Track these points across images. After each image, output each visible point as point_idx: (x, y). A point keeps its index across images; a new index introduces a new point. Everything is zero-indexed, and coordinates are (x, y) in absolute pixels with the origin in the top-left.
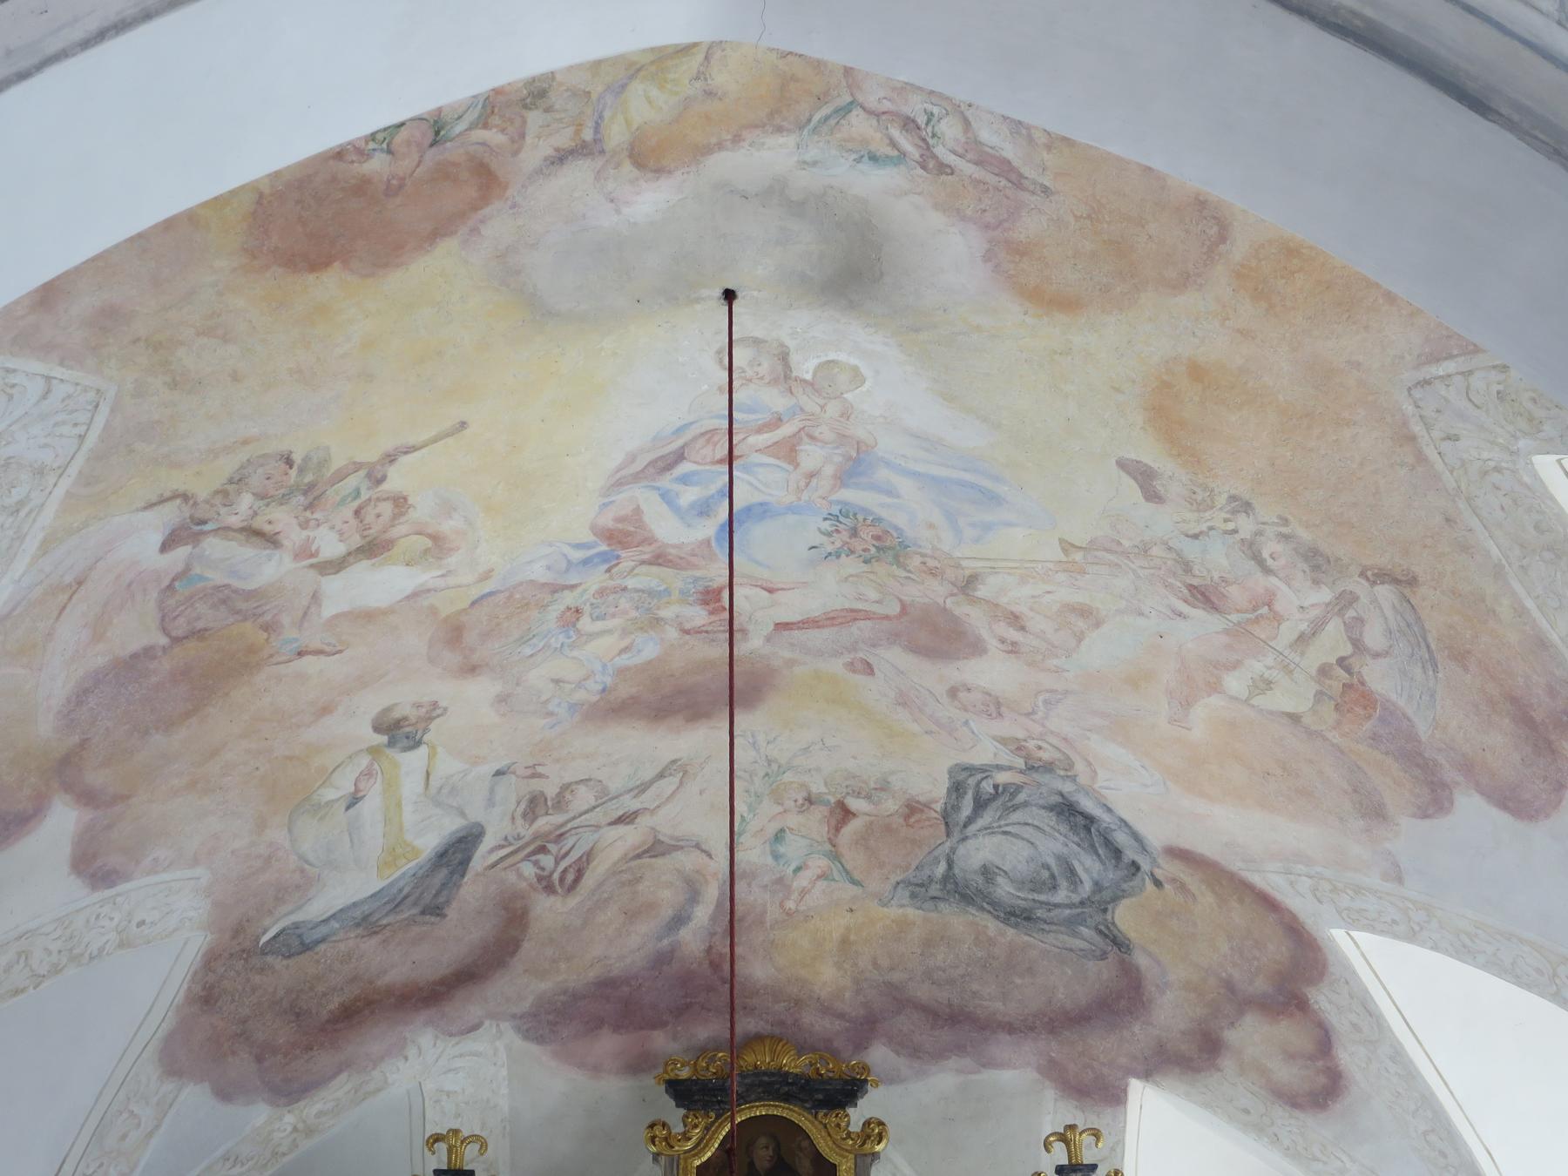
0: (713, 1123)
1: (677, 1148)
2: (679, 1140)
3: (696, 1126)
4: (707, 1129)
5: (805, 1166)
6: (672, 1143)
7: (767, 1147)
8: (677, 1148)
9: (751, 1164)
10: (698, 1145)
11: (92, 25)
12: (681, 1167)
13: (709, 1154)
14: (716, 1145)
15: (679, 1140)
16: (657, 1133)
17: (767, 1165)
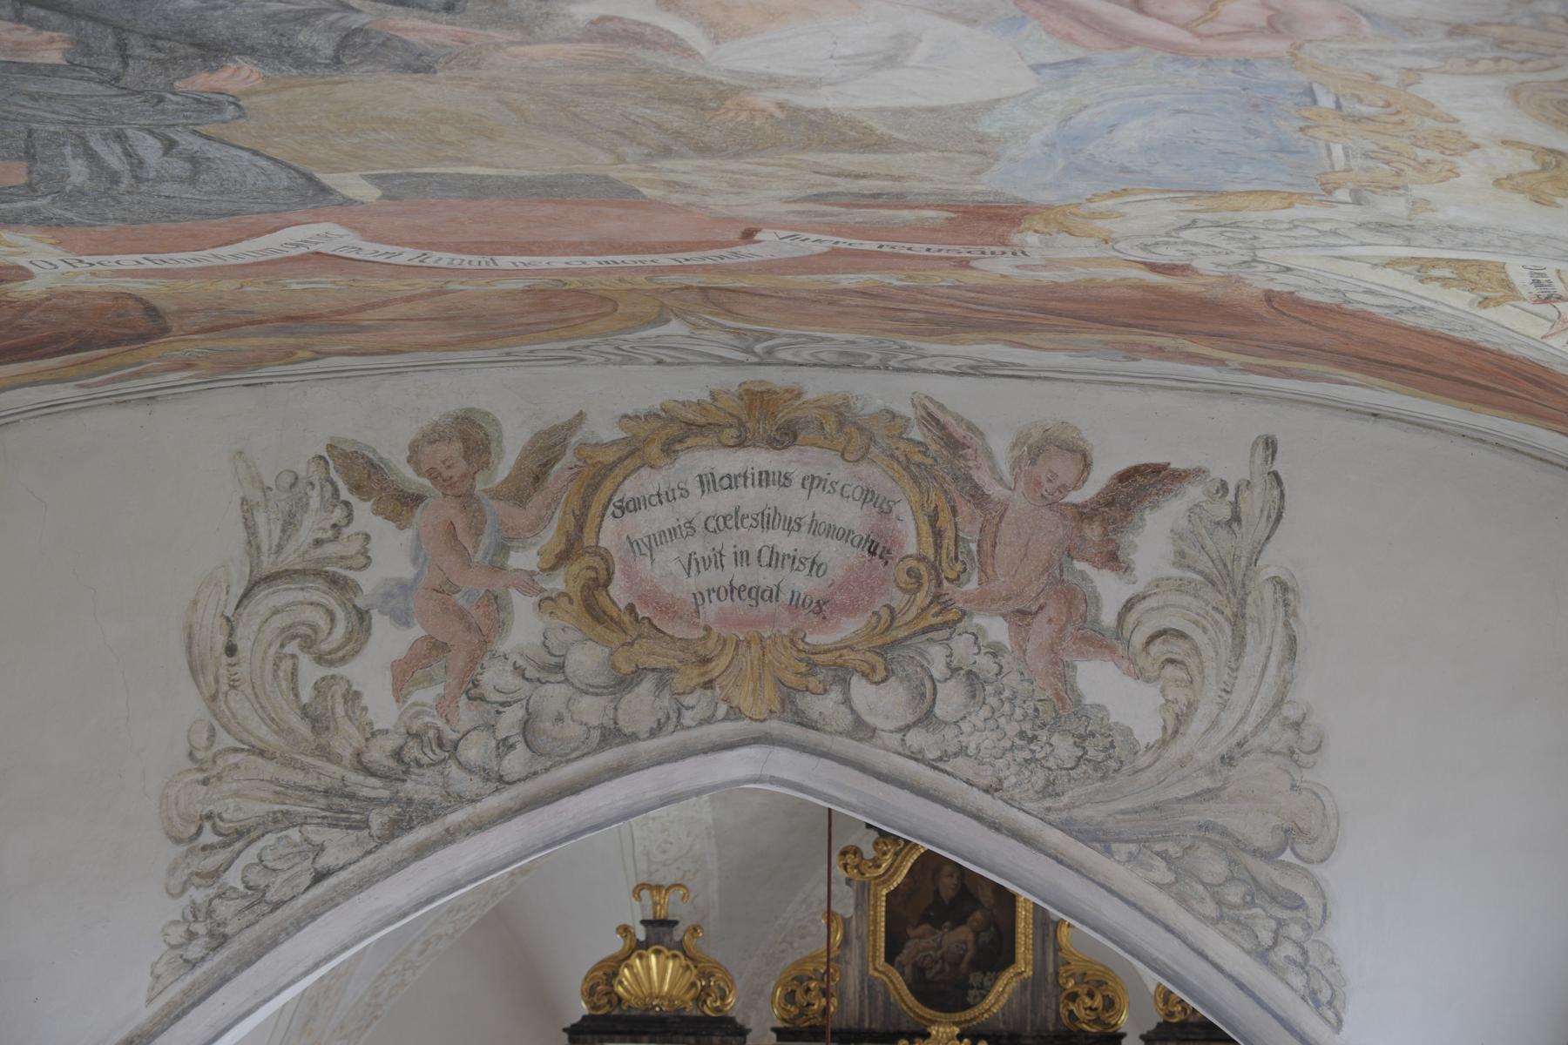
0: (903, 848)
1: (867, 875)
2: (870, 867)
3: (885, 853)
4: (896, 854)
5: (986, 897)
6: (863, 871)
7: (951, 876)
8: (867, 875)
9: (937, 892)
10: (887, 870)
11: (310, 962)
12: (872, 892)
13: (899, 880)
14: (905, 871)
15: (870, 867)
16: (849, 861)
17: (951, 893)
